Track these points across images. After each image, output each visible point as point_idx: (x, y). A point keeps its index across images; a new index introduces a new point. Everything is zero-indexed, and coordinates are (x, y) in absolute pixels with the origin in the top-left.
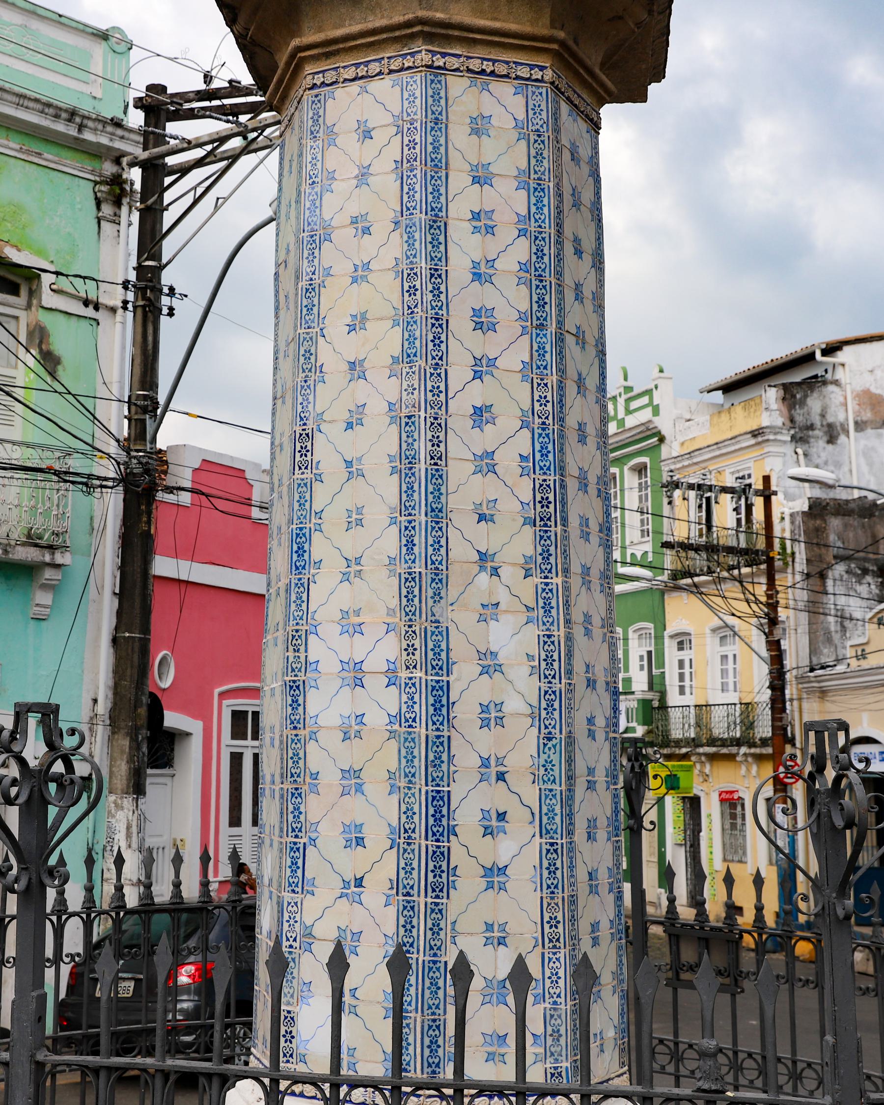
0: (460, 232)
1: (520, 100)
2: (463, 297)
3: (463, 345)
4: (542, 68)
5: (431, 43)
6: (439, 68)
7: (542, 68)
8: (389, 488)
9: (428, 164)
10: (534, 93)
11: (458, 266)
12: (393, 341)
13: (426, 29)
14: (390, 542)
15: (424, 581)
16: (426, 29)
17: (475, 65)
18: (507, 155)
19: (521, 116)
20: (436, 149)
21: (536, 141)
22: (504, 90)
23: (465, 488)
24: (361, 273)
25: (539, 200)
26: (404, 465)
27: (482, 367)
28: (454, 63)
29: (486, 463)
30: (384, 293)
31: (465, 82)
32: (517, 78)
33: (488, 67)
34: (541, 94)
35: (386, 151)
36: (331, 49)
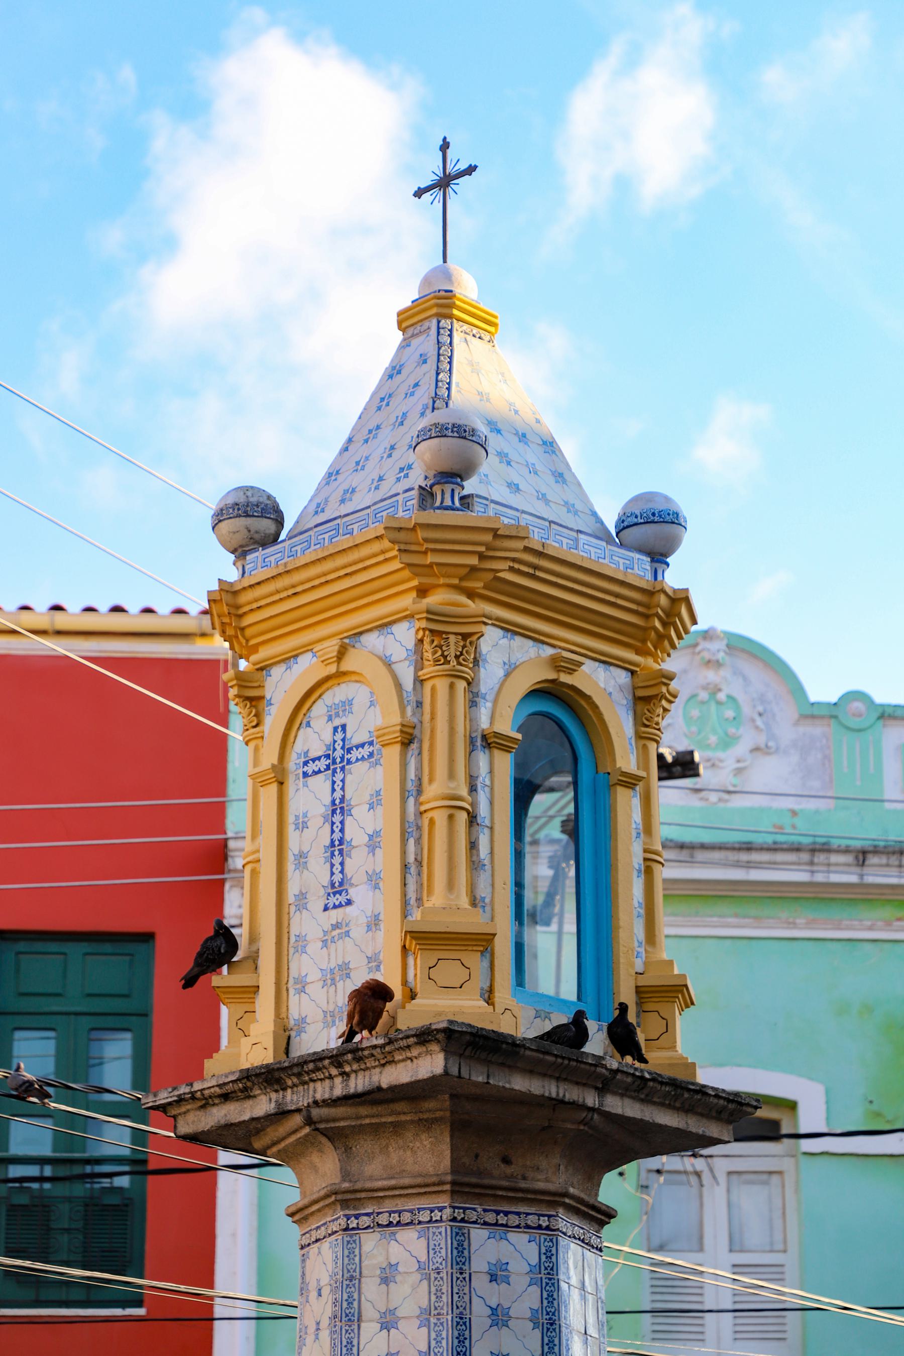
1: (423, 1242)
4: (441, 1209)
5: (348, 1208)
6: (353, 1229)
7: (441, 1209)
10: (434, 1233)
13: (339, 1197)
16: (339, 1197)
17: (383, 1219)
18: (411, 1295)
19: (423, 1258)
20: (350, 1303)
21: (436, 1279)
22: (409, 1236)
25: (439, 1334)
28: (365, 1221)
31: (376, 1236)
32: (420, 1223)
33: (395, 1218)
34: (440, 1233)
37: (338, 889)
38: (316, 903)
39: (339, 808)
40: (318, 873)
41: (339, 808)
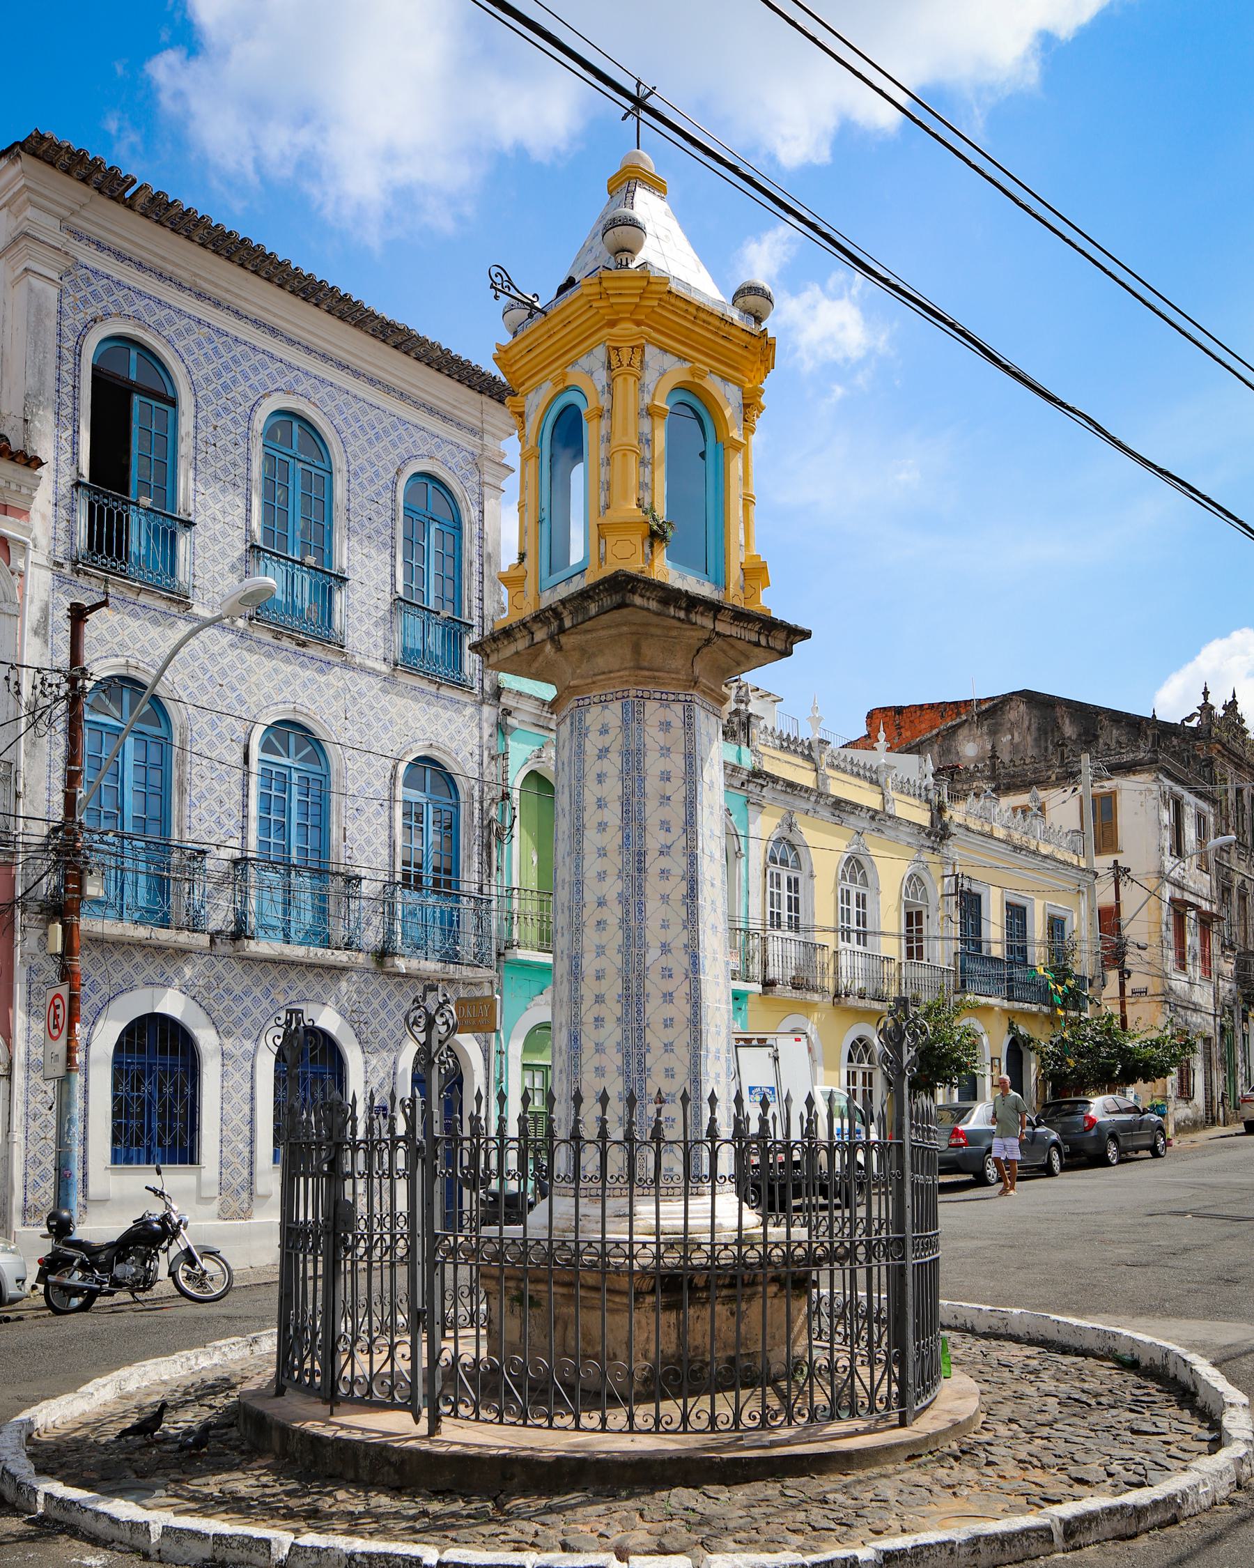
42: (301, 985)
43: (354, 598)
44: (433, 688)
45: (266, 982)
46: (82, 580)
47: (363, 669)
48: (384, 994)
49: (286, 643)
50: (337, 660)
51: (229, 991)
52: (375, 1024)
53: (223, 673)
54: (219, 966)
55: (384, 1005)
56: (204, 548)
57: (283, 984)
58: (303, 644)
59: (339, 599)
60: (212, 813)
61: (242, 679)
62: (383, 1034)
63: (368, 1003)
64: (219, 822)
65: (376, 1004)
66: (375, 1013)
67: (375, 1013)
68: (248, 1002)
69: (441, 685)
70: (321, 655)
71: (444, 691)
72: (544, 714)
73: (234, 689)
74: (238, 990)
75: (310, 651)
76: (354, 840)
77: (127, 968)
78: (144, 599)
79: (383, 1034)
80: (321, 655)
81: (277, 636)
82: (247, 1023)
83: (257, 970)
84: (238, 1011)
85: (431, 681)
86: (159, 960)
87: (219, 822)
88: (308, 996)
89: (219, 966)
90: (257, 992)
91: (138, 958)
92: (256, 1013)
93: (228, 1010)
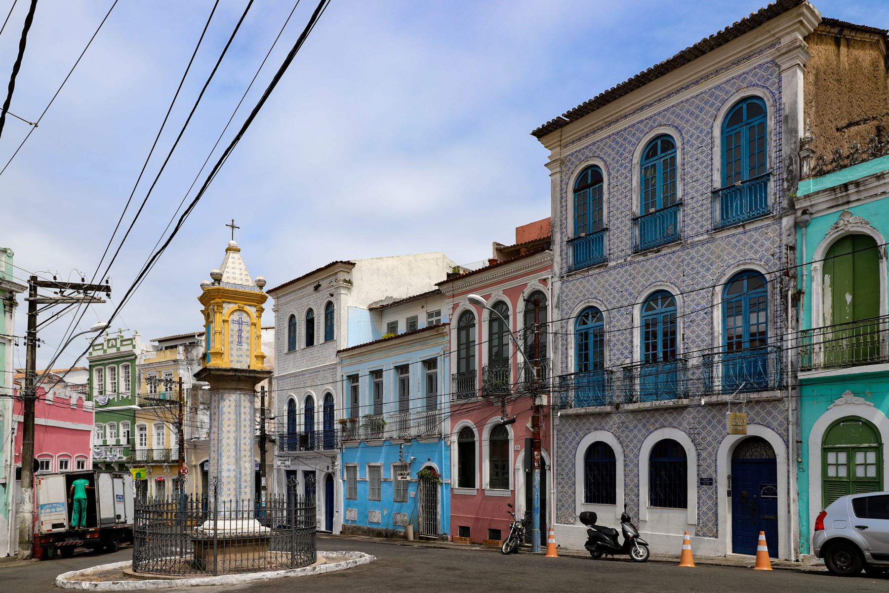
0: (242, 414)
2: (243, 423)
3: (243, 429)
8: (234, 447)
9: (238, 406)
11: (242, 419)
12: (234, 429)
14: (234, 454)
15: (238, 460)
23: (243, 447)
24: (229, 419)
26: (236, 444)
27: (245, 432)
29: (245, 444)
30: (233, 422)
35: (233, 404)
36: (225, 389)
37: (240, 343)
38: (235, 343)
39: (240, 330)
40: (236, 338)
41: (240, 330)
42: (662, 420)
43: (688, 209)
44: (741, 230)
45: (644, 421)
46: (570, 279)
47: (693, 245)
48: (709, 417)
49: (650, 255)
50: (678, 248)
51: (627, 427)
52: (704, 434)
53: (622, 286)
54: (623, 417)
55: (709, 422)
56: (613, 235)
57: (652, 420)
58: (658, 251)
59: (680, 216)
60: (619, 350)
61: (631, 284)
62: (709, 439)
63: (699, 423)
64: (622, 354)
65: (704, 423)
66: (704, 428)
67: (704, 428)
68: (635, 431)
69: (743, 226)
70: (669, 251)
71: (748, 228)
72: (840, 195)
73: (627, 290)
74: (631, 427)
75: (663, 252)
76: (688, 338)
77: (588, 425)
78: (591, 272)
79: (709, 439)
80: (669, 251)
81: (645, 255)
82: (635, 441)
83: (640, 416)
84: (631, 436)
85: (735, 228)
86: (599, 419)
87: (622, 354)
88: (666, 424)
89: (623, 417)
90: (640, 426)
91: (592, 420)
92: (640, 436)
93: (627, 436)
